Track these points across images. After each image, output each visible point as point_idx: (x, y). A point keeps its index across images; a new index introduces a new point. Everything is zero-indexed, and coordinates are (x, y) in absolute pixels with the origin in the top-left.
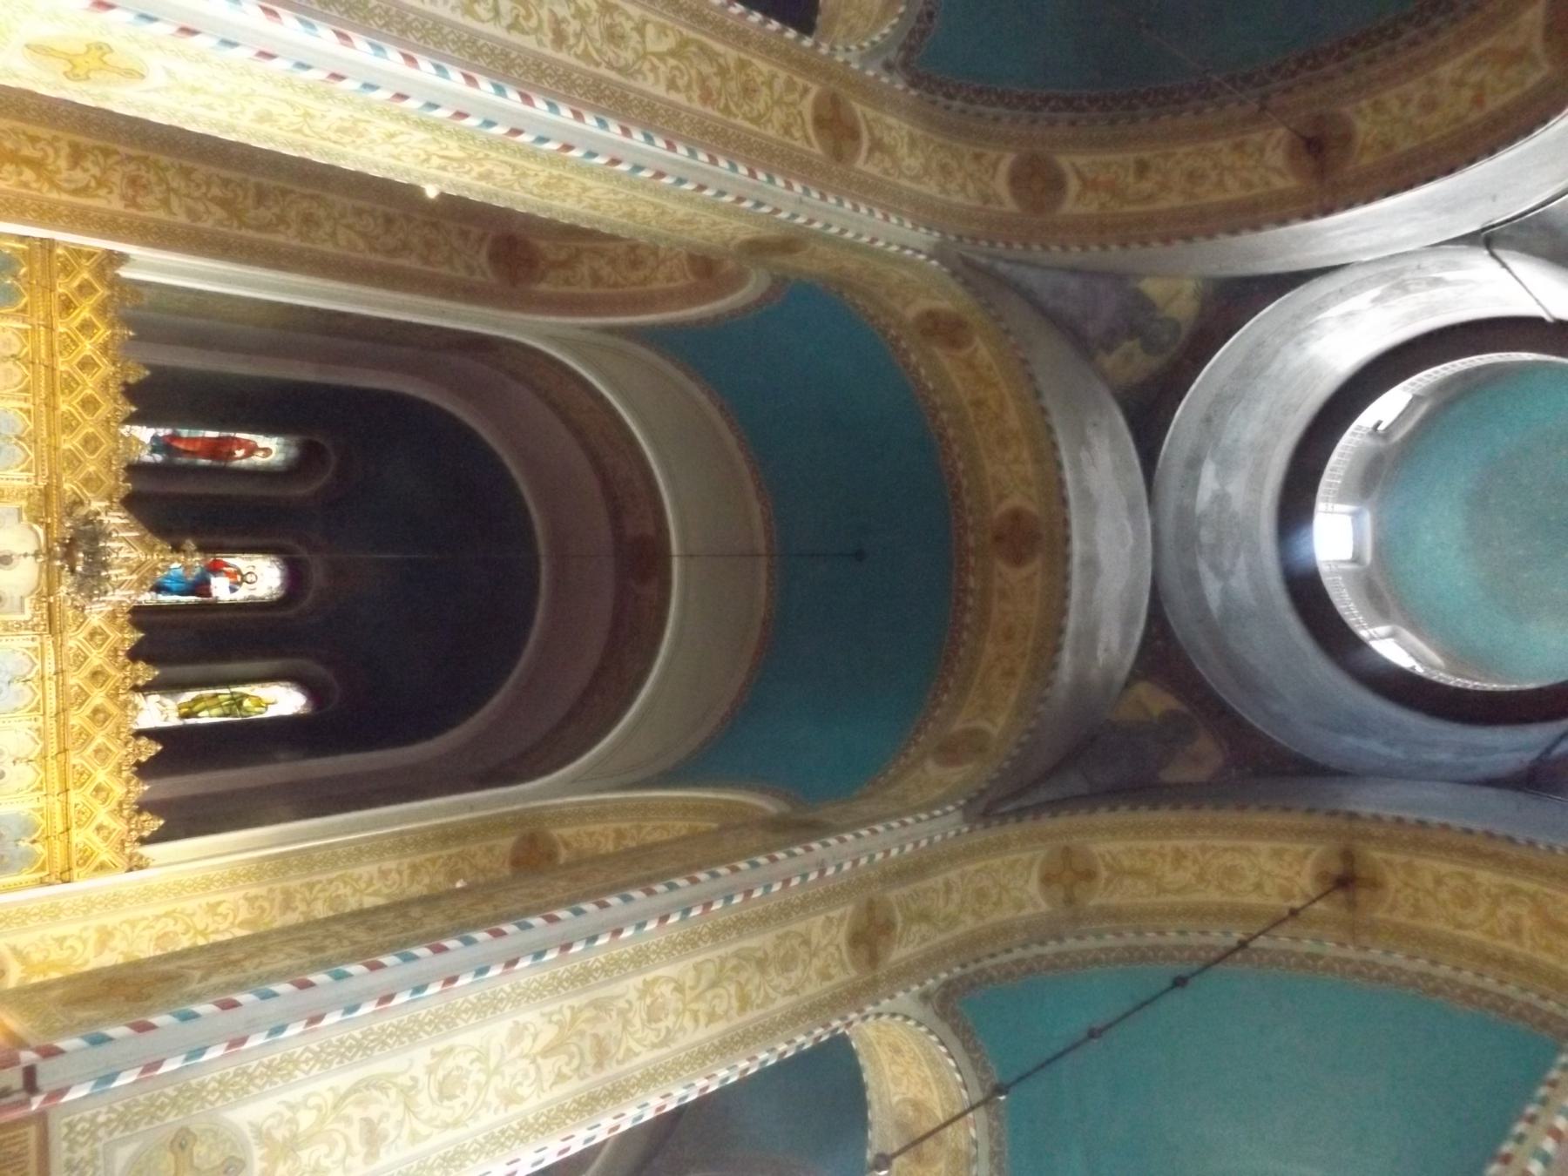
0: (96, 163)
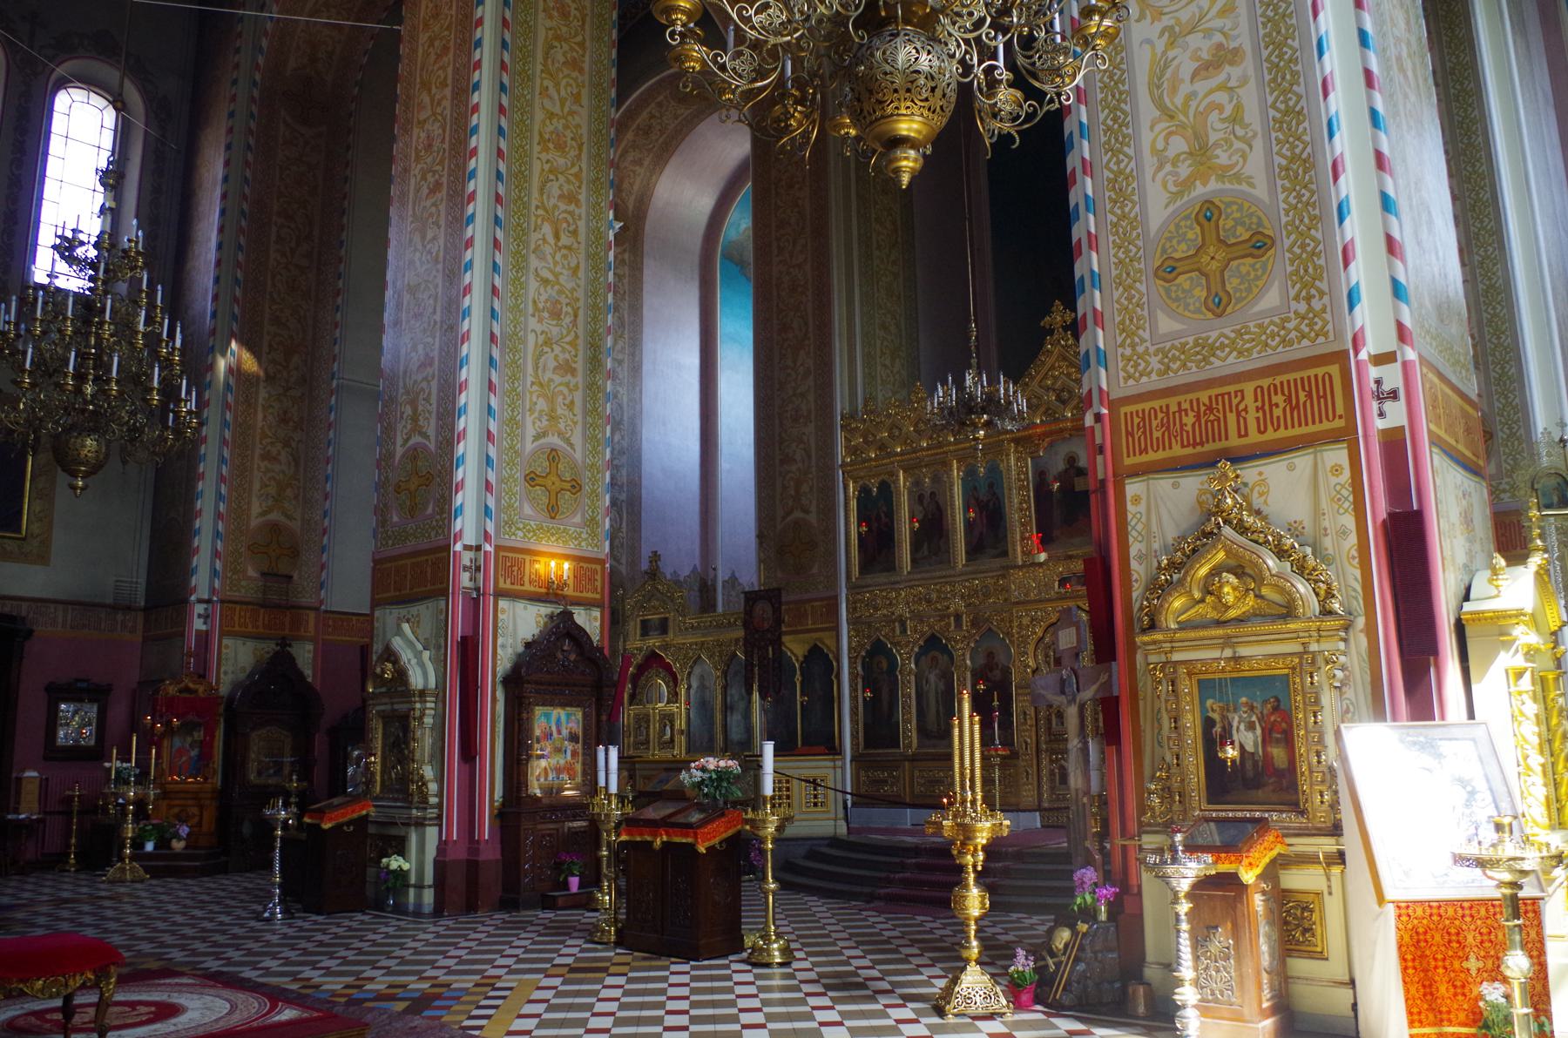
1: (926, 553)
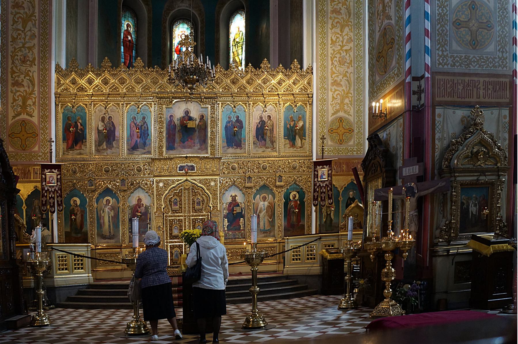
0: (19, 76)
1: (105, 147)
